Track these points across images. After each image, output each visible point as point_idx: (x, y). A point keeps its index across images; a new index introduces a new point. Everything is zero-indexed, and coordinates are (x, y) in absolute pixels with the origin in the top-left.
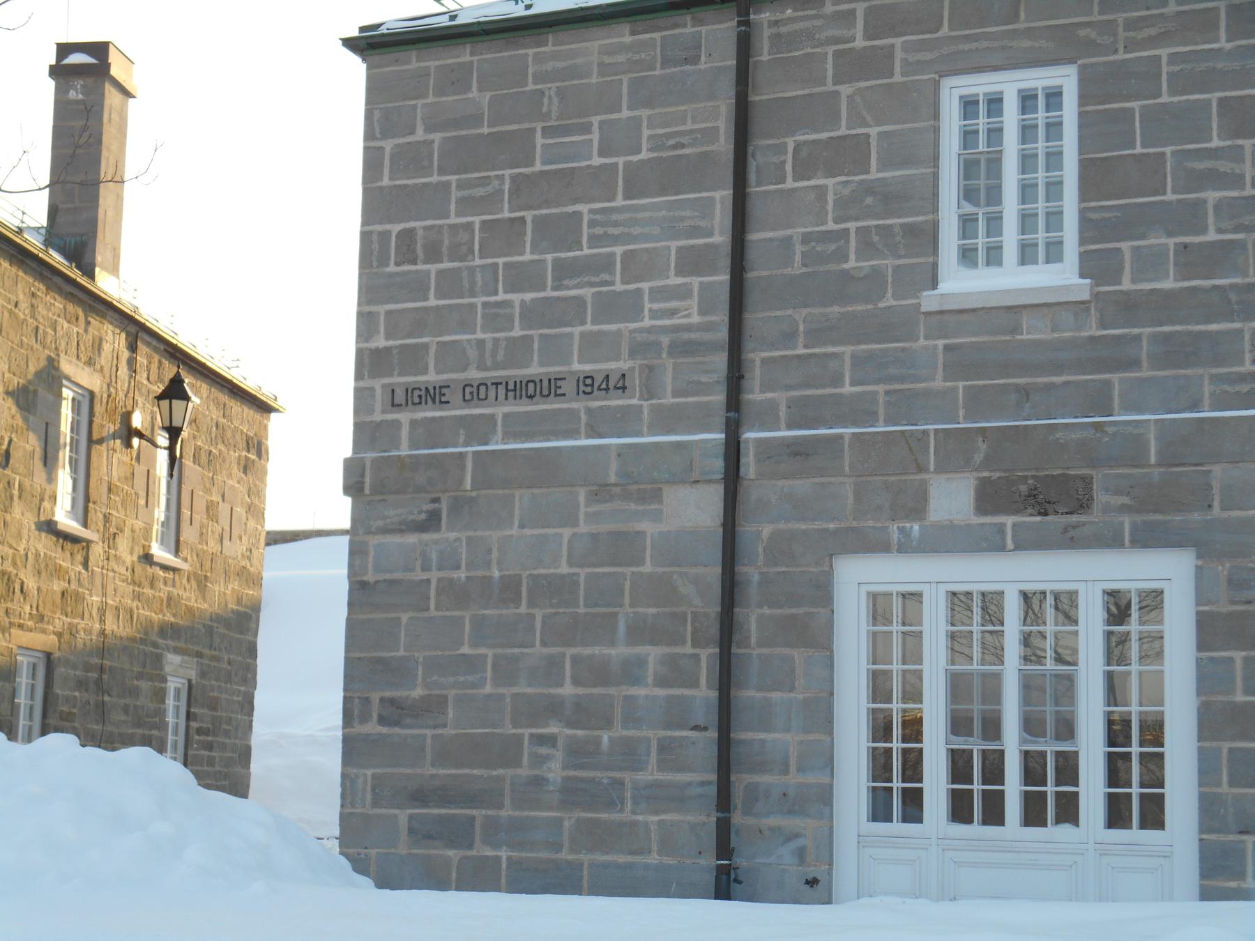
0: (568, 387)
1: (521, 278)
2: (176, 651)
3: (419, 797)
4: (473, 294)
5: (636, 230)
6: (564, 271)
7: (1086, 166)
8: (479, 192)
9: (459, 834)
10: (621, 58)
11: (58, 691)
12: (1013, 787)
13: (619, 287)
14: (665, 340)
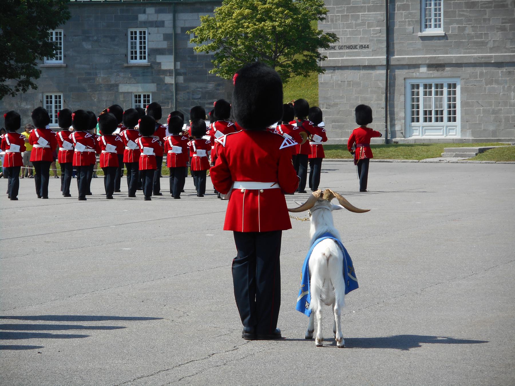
1: (349, 26)
3: (334, 121)
4: (340, 29)
5: (370, 18)
6: (357, 25)
7: (444, 12)
8: (340, 9)
9: (341, 127)
12: (433, 116)
14: (375, 39)
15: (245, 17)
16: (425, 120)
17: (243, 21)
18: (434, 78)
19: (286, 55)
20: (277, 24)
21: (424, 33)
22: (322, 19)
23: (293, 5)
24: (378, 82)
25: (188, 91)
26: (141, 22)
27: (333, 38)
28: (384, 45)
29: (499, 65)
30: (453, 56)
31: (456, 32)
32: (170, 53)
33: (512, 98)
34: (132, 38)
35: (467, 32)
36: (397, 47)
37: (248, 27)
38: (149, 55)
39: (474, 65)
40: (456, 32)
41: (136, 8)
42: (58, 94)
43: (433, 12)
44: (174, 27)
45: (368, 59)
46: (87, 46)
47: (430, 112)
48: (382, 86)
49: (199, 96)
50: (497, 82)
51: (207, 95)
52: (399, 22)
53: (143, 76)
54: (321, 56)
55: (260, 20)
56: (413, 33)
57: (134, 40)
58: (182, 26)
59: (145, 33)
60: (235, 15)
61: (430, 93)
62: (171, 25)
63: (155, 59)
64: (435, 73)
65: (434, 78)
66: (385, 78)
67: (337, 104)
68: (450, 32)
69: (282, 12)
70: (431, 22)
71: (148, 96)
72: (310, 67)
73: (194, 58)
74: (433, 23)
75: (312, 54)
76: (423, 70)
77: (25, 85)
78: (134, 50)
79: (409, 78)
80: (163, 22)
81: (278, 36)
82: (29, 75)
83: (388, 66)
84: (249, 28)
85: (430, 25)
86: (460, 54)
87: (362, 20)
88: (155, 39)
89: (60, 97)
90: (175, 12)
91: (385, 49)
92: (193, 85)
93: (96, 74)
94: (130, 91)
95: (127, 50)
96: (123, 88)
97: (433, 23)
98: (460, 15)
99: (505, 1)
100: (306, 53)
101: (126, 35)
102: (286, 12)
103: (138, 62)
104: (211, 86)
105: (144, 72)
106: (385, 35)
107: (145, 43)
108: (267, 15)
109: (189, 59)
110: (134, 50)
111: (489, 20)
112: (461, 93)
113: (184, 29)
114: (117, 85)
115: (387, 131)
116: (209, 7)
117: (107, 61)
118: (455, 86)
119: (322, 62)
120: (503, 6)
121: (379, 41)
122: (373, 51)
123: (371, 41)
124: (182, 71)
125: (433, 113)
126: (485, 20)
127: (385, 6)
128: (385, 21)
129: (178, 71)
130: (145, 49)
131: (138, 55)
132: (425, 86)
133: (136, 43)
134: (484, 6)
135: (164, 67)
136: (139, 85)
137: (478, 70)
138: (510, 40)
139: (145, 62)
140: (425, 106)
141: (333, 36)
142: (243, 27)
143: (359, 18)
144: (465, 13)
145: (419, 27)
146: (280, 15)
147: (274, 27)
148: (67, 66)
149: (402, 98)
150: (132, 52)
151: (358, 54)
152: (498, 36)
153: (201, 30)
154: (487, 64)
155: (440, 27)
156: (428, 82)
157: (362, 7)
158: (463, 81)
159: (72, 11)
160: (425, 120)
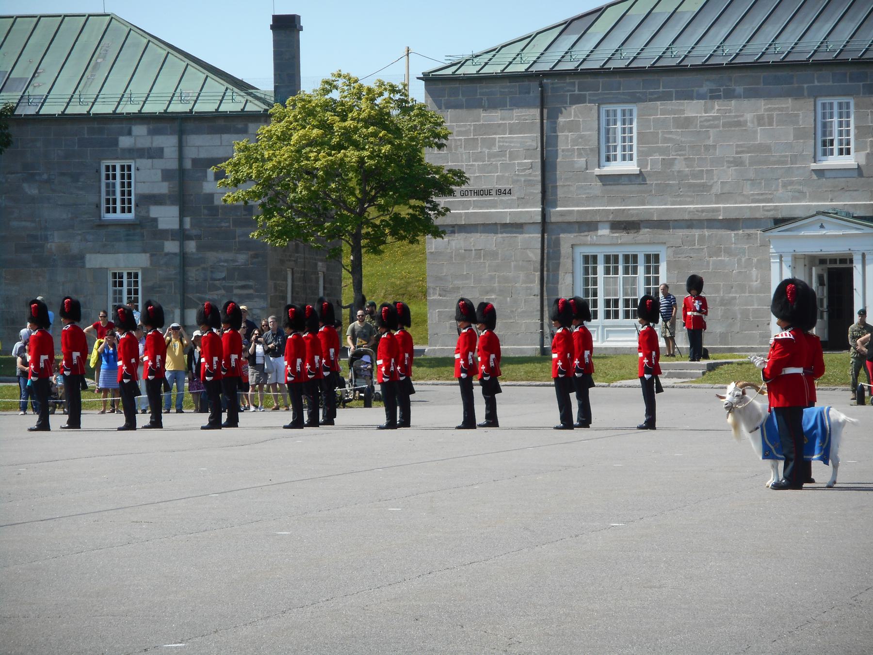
0: (493, 192)
2: (322, 261)
6: (491, 156)
7: (639, 133)
8: (463, 129)
10: (506, 90)
11: (296, 283)
12: (621, 308)
13: (508, 162)
14: (523, 179)
15: (312, 143)
16: (608, 315)
17: (308, 149)
18: (621, 244)
19: (380, 208)
20: (366, 153)
21: (606, 169)
22: (440, 146)
23: (392, 122)
24: (528, 251)
25: (203, 265)
26: (123, 150)
27: (460, 177)
28: (538, 188)
29: (731, 224)
30: (654, 208)
31: (659, 167)
32: (172, 204)
33: (754, 278)
34: (108, 177)
35: (676, 168)
36: (560, 193)
37: (316, 160)
38: (137, 205)
39: (690, 224)
40: (659, 167)
41: (115, 126)
43: (619, 135)
44: (181, 158)
45: (510, 213)
46: (31, 190)
47: (616, 302)
48: (534, 259)
49: (223, 275)
50: (729, 252)
51: (236, 274)
52: (563, 150)
53: (127, 240)
54: (440, 208)
55: (339, 147)
56: (587, 169)
57: (111, 181)
58: (193, 157)
59: (129, 167)
60: (295, 137)
61: (616, 272)
62: (175, 155)
63: (148, 212)
64: (623, 236)
65: (621, 244)
66: (539, 245)
67: (458, 288)
68: (649, 169)
69: (374, 134)
70: (615, 151)
71: (136, 276)
72: (419, 226)
73: (214, 210)
74: (619, 152)
75: (425, 204)
76: (604, 231)
78: (111, 197)
79: (580, 245)
80: (161, 150)
81: (366, 175)
83: (545, 224)
84: (320, 160)
85: (615, 156)
86: (665, 204)
87: (500, 147)
88: (148, 178)
90: (181, 134)
91: (540, 196)
92: (212, 257)
93: (46, 238)
94: (105, 266)
95: (100, 196)
96: (94, 261)
97: (619, 152)
98: (666, 140)
99: (742, 116)
100: (413, 202)
101: (98, 171)
102: (381, 135)
103: (119, 216)
104: (242, 258)
105: (128, 235)
106: (539, 172)
107: (129, 184)
108: (348, 139)
109: (206, 212)
110: (111, 197)
111: (714, 147)
112: (668, 270)
113: (195, 161)
114: (82, 258)
115: (542, 334)
116: (240, 126)
117: (64, 216)
118: (657, 257)
119: (440, 218)
120: (739, 124)
121: (529, 183)
122: (518, 199)
123: (515, 182)
124: (194, 232)
125: (621, 303)
126: (707, 148)
127: (539, 125)
128: (539, 149)
129: (187, 232)
130: (130, 194)
131: (119, 205)
132: (607, 259)
133: (114, 185)
134: (706, 124)
135: (162, 226)
137: (696, 233)
138: (749, 182)
139: (130, 216)
140: (607, 293)
141: (459, 174)
142: (308, 159)
143: (494, 144)
144: (674, 137)
145: (597, 159)
146: (371, 139)
147: (361, 161)
149: (568, 279)
150: (108, 201)
151: (494, 205)
152: (730, 174)
153: (235, 165)
154: (712, 223)
155: (631, 160)
156: (612, 251)
157: (499, 125)
158: (670, 250)
160: (608, 315)
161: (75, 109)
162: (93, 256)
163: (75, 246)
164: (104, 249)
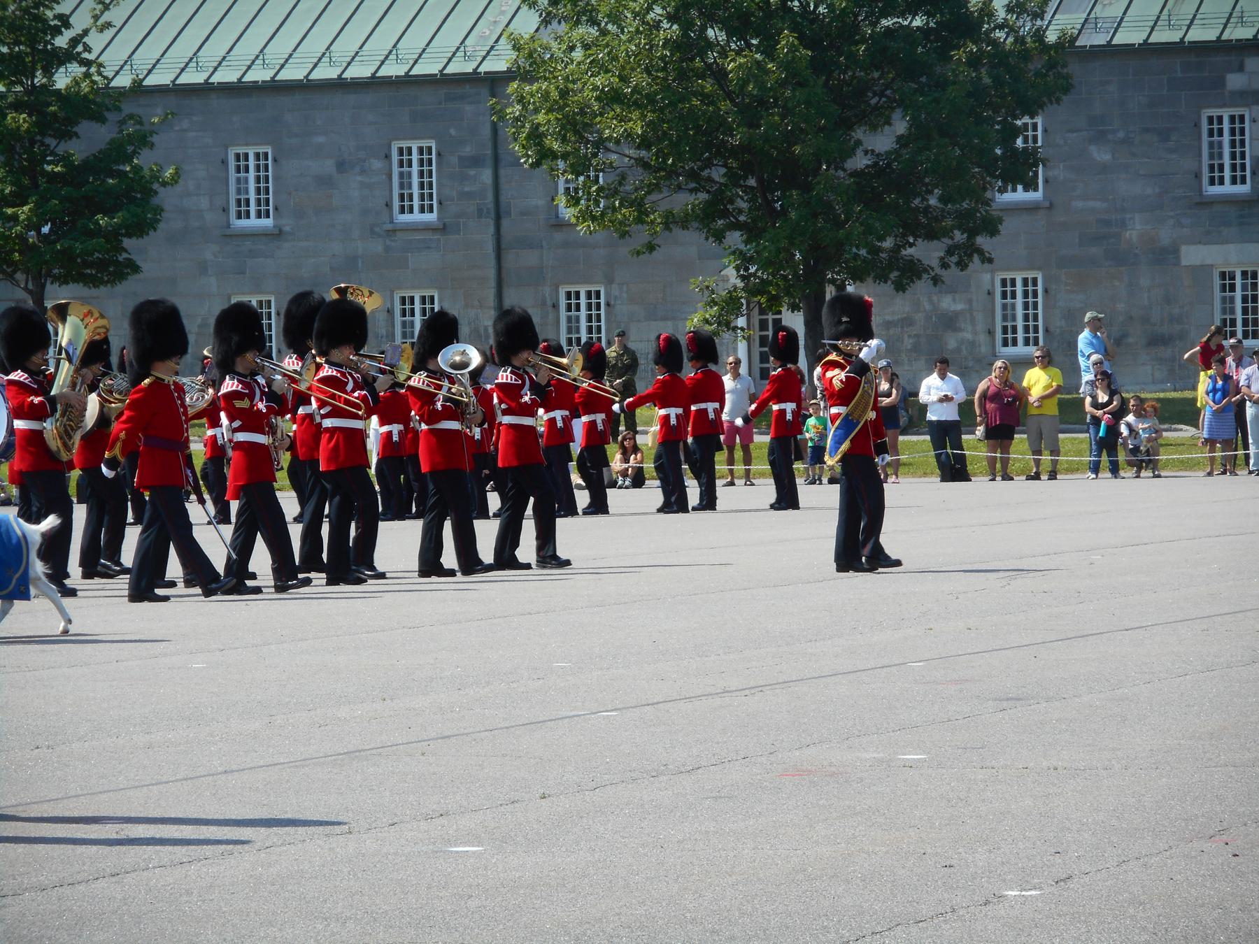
26: (1233, 93)
34: (1211, 133)
38: (1253, 173)
42: (1030, 275)
46: (1102, 155)
57: (1216, 138)
59: (1242, 118)
77: (965, 254)
78: (1216, 162)
82: (973, 233)
89: (1035, 281)
93: (1123, 224)
94: (1209, 262)
95: (1200, 162)
96: (1193, 255)
101: (1197, 125)
103: (1228, 188)
107: (1243, 143)
110: (1216, 162)
114: (1175, 251)
117: (1149, 191)
130: (1243, 157)
131: (1227, 174)
136: (1231, 247)
148: (1051, 207)
150: (1212, 168)
159: (1074, 68)
161: (1160, 37)
162: (1192, 248)
163: (1165, 235)
164: (1207, 238)
